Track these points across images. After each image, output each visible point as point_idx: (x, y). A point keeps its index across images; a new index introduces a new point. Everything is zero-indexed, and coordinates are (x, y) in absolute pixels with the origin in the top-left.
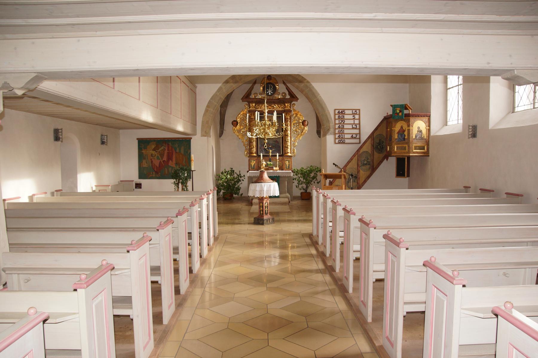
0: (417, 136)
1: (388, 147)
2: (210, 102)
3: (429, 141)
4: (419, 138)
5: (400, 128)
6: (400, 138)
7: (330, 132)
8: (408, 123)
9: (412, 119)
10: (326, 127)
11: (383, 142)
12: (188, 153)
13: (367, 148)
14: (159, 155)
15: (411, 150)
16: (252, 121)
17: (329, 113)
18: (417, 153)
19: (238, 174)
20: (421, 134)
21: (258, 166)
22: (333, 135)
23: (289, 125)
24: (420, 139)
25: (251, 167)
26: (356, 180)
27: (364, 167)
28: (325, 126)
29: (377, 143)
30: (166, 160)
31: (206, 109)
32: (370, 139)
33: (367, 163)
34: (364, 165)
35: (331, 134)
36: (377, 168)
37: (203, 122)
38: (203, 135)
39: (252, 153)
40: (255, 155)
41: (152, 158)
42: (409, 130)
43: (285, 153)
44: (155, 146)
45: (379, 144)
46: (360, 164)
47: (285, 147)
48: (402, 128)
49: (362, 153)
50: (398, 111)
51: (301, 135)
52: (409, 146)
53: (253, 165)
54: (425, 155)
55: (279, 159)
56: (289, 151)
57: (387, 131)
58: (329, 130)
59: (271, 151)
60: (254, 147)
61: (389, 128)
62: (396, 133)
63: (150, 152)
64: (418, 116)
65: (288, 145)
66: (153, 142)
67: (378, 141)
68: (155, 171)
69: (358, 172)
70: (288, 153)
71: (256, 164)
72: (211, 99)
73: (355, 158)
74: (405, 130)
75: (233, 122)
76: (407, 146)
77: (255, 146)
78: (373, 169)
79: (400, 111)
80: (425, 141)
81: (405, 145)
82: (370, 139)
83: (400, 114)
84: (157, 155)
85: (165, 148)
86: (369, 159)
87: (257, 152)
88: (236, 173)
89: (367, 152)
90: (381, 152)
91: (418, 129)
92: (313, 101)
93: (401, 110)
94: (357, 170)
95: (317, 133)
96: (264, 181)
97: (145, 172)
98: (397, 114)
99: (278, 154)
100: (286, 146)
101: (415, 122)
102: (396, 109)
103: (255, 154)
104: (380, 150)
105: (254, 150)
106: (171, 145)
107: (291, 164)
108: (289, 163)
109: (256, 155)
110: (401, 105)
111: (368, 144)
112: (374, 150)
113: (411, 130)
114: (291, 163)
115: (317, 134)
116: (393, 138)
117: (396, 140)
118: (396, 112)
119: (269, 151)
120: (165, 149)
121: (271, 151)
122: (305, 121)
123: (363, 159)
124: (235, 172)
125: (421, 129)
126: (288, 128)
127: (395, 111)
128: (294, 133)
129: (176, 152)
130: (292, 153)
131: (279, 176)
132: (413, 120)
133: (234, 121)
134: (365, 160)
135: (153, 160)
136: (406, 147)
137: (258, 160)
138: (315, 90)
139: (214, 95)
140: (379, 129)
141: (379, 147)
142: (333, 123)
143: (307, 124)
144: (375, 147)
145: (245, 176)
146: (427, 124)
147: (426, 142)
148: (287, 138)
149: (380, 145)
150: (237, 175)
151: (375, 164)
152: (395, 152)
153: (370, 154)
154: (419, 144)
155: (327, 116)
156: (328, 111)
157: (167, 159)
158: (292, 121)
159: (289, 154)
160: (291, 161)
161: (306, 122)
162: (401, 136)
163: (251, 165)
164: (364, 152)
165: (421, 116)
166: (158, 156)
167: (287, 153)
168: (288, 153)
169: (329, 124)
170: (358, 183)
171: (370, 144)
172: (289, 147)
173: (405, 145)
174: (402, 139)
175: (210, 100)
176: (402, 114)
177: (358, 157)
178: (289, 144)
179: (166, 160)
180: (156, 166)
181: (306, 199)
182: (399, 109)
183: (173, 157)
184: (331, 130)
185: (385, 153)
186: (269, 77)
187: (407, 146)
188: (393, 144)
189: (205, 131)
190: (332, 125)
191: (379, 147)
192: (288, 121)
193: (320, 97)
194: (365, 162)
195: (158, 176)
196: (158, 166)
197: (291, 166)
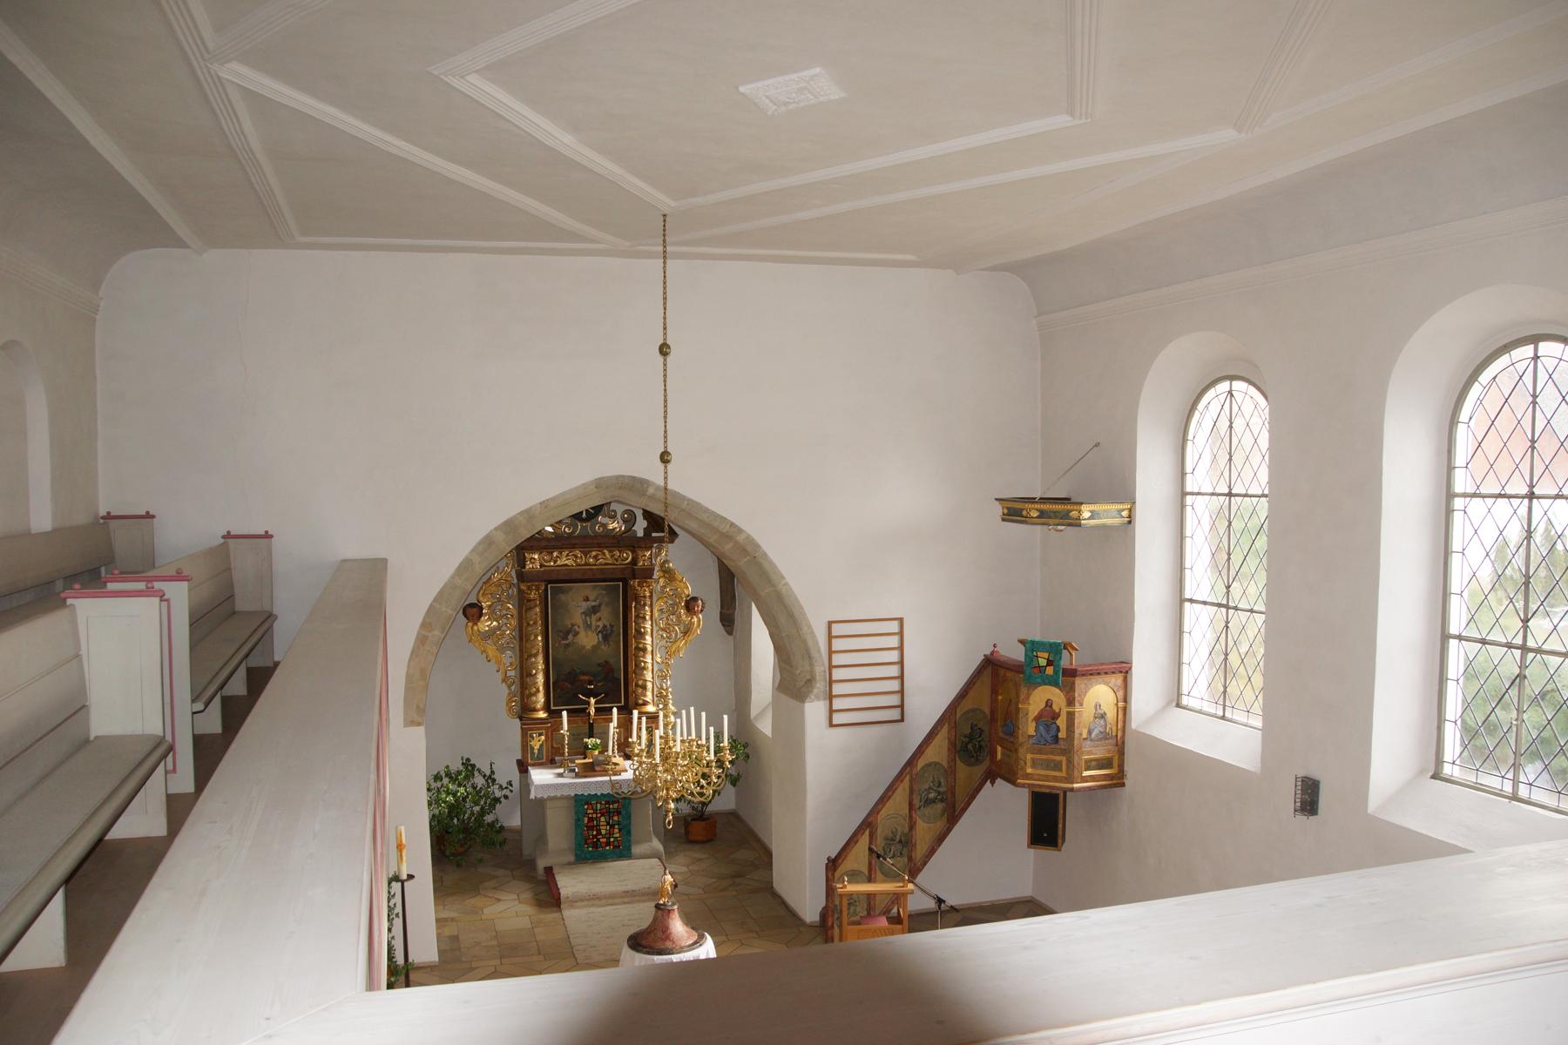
0: (1093, 730)
1: (999, 748)
2: (431, 610)
3: (1123, 743)
4: (1097, 735)
5: (1043, 705)
6: (1042, 735)
7: (815, 690)
8: (1068, 693)
9: (1079, 683)
10: (799, 674)
11: (982, 731)
13: (938, 752)
15: (1076, 773)
16: (531, 609)
17: (812, 632)
18: (1092, 778)
20: (1102, 722)
22: (824, 700)
23: (648, 617)
24: (1100, 739)
25: (533, 753)
26: (905, 851)
27: (927, 811)
28: (798, 672)
29: (965, 737)
31: (419, 633)
32: (947, 724)
33: (936, 798)
34: (928, 802)
35: (818, 698)
36: (964, 810)
37: (408, 676)
38: (410, 723)
39: (535, 710)
40: (542, 715)
42: (1071, 716)
45: (971, 737)
46: (916, 803)
48: (1051, 706)
49: (923, 768)
50: (1043, 662)
52: (1070, 762)
53: (537, 747)
54: (1115, 782)
56: (649, 694)
57: (994, 702)
58: (810, 682)
59: (593, 701)
60: (538, 691)
61: (1000, 692)
62: (1030, 720)
64: (1099, 674)
67: (968, 731)
69: (912, 827)
72: (435, 600)
73: (902, 785)
74: (1060, 712)
75: (469, 611)
76: (1064, 759)
77: (541, 688)
78: (953, 816)
79: (1050, 663)
80: (1115, 741)
81: (1058, 758)
82: (947, 724)
83: (1050, 671)
86: (943, 784)
87: (547, 708)
88: (479, 770)
89: (939, 763)
90: (977, 760)
91: (1096, 710)
92: (763, 594)
93: (1051, 659)
94: (907, 819)
95: (722, 620)
96: (674, 943)
98: (1041, 669)
100: (640, 683)
101: (1089, 689)
102: (1035, 654)
104: (973, 756)
105: (541, 699)
110: (1051, 645)
111: (941, 741)
112: (955, 760)
113: (1077, 714)
115: (723, 625)
116: (1020, 732)
117: (1031, 741)
118: (1035, 664)
119: (588, 703)
121: (593, 701)
122: (695, 599)
123: (927, 786)
125: (1105, 708)
126: (644, 628)
127: (1032, 660)
128: (662, 636)
132: (1083, 686)
133: (471, 605)
134: (930, 788)
136: (1061, 762)
138: (771, 563)
139: (446, 585)
140: (971, 693)
141: (970, 746)
142: (823, 665)
144: (958, 748)
145: (511, 785)
146: (1121, 694)
147: (1117, 745)
148: (644, 657)
149: (974, 742)
150: (484, 776)
151: (960, 796)
152: (1027, 776)
153: (946, 770)
154: (1099, 752)
155: (804, 642)
156: (810, 627)
161: (700, 601)
162: (1048, 731)
163: (532, 749)
164: (929, 765)
165: (1106, 673)
168: (645, 703)
169: (811, 665)
170: (910, 859)
171: (947, 741)
172: (649, 685)
173: (1058, 758)
174: (1049, 739)
175: (431, 605)
176: (1056, 672)
177: (911, 781)
178: (648, 676)
181: (703, 842)
182: (1046, 655)
184: (818, 685)
185: (986, 764)
187: (1064, 759)
188: (1022, 751)
189: (418, 707)
190: (822, 668)
191: (971, 748)
192: (645, 605)
193: (786, 584)
194: (932, 795)
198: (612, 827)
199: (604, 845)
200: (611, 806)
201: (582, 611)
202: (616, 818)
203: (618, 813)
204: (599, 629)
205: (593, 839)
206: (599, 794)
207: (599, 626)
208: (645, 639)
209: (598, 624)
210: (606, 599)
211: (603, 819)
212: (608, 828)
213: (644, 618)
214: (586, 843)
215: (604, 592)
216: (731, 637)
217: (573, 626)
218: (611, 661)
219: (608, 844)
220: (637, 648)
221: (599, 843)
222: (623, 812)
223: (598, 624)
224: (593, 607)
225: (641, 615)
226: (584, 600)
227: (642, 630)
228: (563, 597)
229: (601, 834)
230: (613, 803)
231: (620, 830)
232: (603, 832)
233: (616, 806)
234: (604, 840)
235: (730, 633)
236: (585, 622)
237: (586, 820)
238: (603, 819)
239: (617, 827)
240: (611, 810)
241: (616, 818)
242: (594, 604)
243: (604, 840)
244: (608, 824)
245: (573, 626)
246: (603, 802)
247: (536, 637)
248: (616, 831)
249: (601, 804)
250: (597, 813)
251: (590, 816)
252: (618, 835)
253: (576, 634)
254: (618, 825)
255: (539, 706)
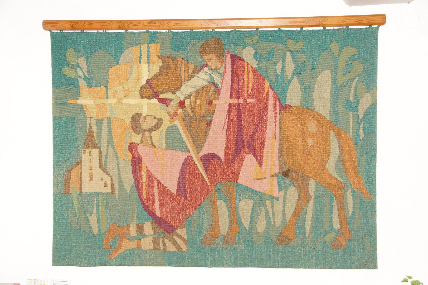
12: (361, 112)
14: (177, 123)
30: (221, 154)
41: (136, 139)
44: (155, 70)
63: (125, 101)
66: (144, 47)
68: (152, 214)
84: (166, 123)
85: (217, 79)
97: (93, 219)
106: (254, 64)
120: (218, 91)
129: (284, 107)
135: (141, 150)
157: (227, 146)
166: (172, 130)
179: (221, 154)
180: (160, 185)
183: (264, 133)
195: (171, 248)
196: (173, 189)
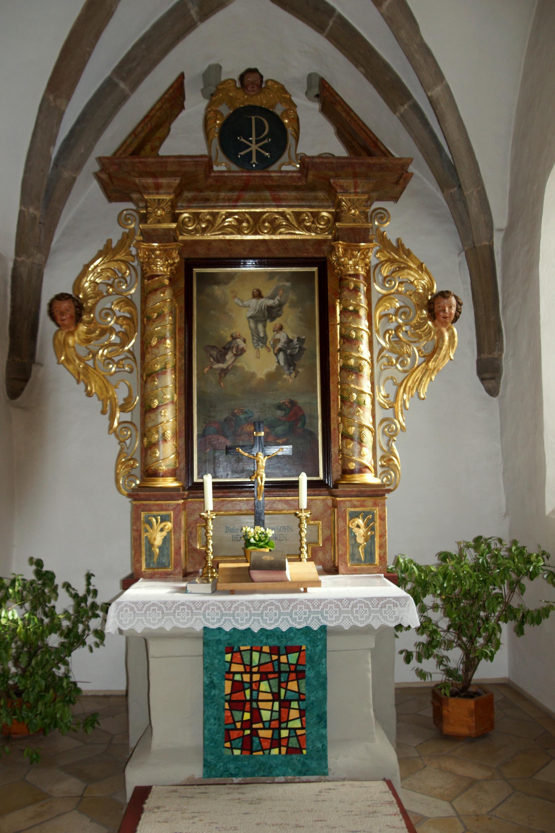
19: (81, 592)
21: (191, 550)
25: (150, 554)
40: (170, 483)
43: (346, 472)
47: (346, 436)
51: (426, 371)
55: (309, 508)
56: (367, 452)
65: (361, 426)
70: (362, 469)
71: (178, 540)
77: (169, 434)
88: (67, 586)
95: (480, 372)
99: (303, 479)
100: (352, 430)
103: (170, 479)
107: (382, 536)
108: (373, 529)
109: (176, 484)
114: (383, 526)
115: (482, 380)
122: (444, 295)
124: (59, 581)
126: (357, 330)
130: (380, 470)
131: (323, 628)
137: (188, 516)
143: (453, 311)
150: (75, 596)
158: (374, 300)
159: (369, 478)
160: (382, 518)
163: (150, 545)
167: (352, 472)
168: (362, 469)
172: (368, 437)
181: (470, 739)
186: (251, 78)
197: (382, 546)
198: (285, 704)
199: (266, 745)
200: (283, 659)
201: (250, 314)
202: (293, 686)
203: (300, 675)
204: (279, 346)
205: (243, 729)
206: (256, 630)
207: (279, 340)
208: (358, 351)
209: (278, 336)
210: (292, 296)
211: (264, 686)
212: (276, 705)
213: (356, 313)
214: (228, 739)
215: (288, 284)
216: (495, 400)
217: (234, 338)
218: (301, 401)
219: (276, 742)
220: (346, 369)
221: (256, 740)
222: (310, 674)
223: (278, 336)
224: (270, 308)
225: (351, 308)
226: (254, 296)
227: (354, 334)
228: (217, 290)
229: (260, 720)
230: (289, 650)
231: (302, 713)
232: (266, 715)
233: (293, 658)
234: (266, 734)
235: (493, 392)
236: (255, 333)
237: (228, 686)
238: (264, 686)
239: (294, 705)
240: (284, 668)
241: (293, 686)
242: (270, 302)
243: (266, 734)
244: (276, 697)
245: (234, 338)
246: (266, 649)
247: (162, 339)
248: (294, 714)
249: (261, 652)
250: (251, 673)
251: (238, 677)
252: (297, 724)
253: (240, 352)
254: (298, 700)
255: (164, 467)
